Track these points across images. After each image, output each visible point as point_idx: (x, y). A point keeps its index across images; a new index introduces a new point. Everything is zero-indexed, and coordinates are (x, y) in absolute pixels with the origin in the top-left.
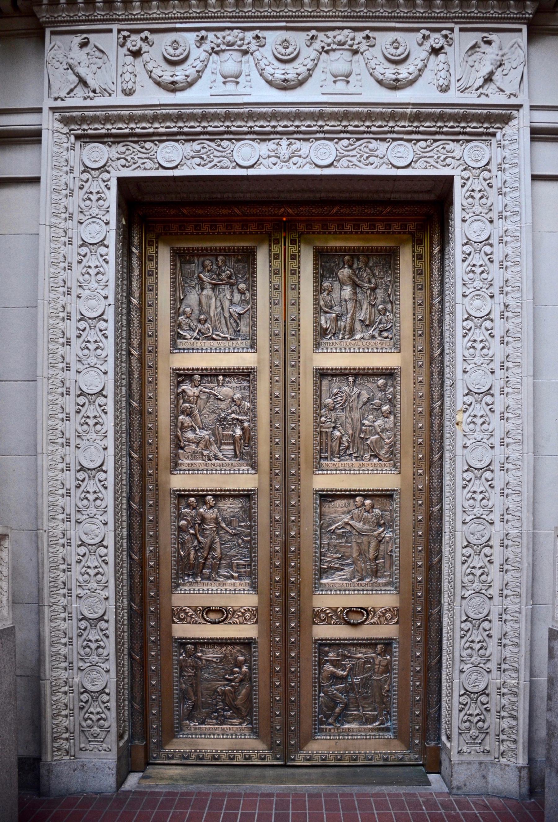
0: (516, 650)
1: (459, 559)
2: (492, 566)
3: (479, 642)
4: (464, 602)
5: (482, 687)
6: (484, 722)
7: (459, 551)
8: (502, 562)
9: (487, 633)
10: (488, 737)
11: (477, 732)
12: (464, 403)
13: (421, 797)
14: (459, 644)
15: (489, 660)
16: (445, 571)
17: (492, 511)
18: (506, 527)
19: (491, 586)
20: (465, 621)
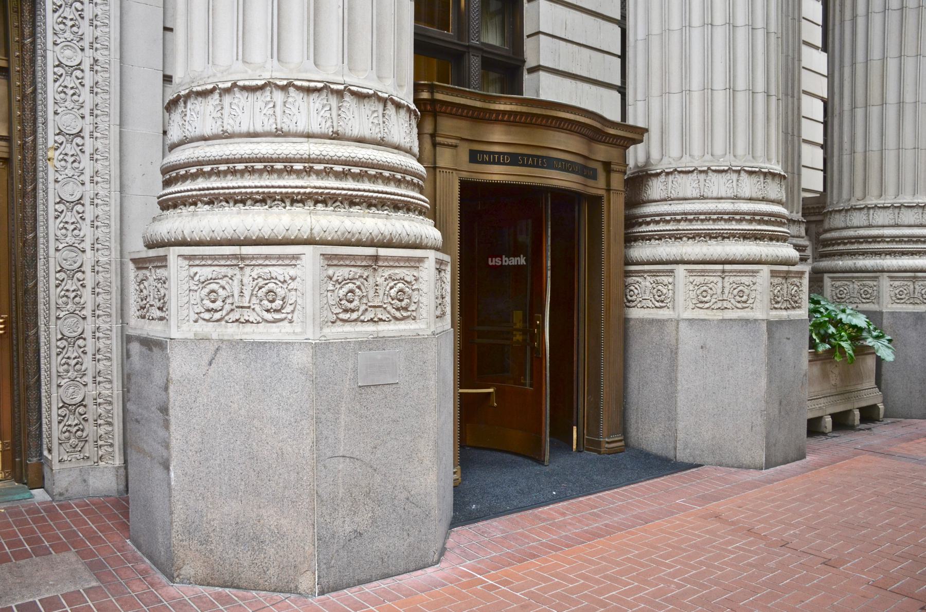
0: (109, 364)
1: (53, 282)
2: (85, 290)
3: (74, 358)
4: (59, 322)
5: (78, 399)
6: (82, 431)
7: (52, 276)
8: (93, 286)
9: (82, 349)
10: (87, 445)
11: (77, 440)
12: (56, 142)
13: (23, 507)
14: (55, 361)
15: (85, 374)
16: (41, 295)
17: (83, 241)
18: (96, 255)
19: (84, 308)
20: (61, 339)
